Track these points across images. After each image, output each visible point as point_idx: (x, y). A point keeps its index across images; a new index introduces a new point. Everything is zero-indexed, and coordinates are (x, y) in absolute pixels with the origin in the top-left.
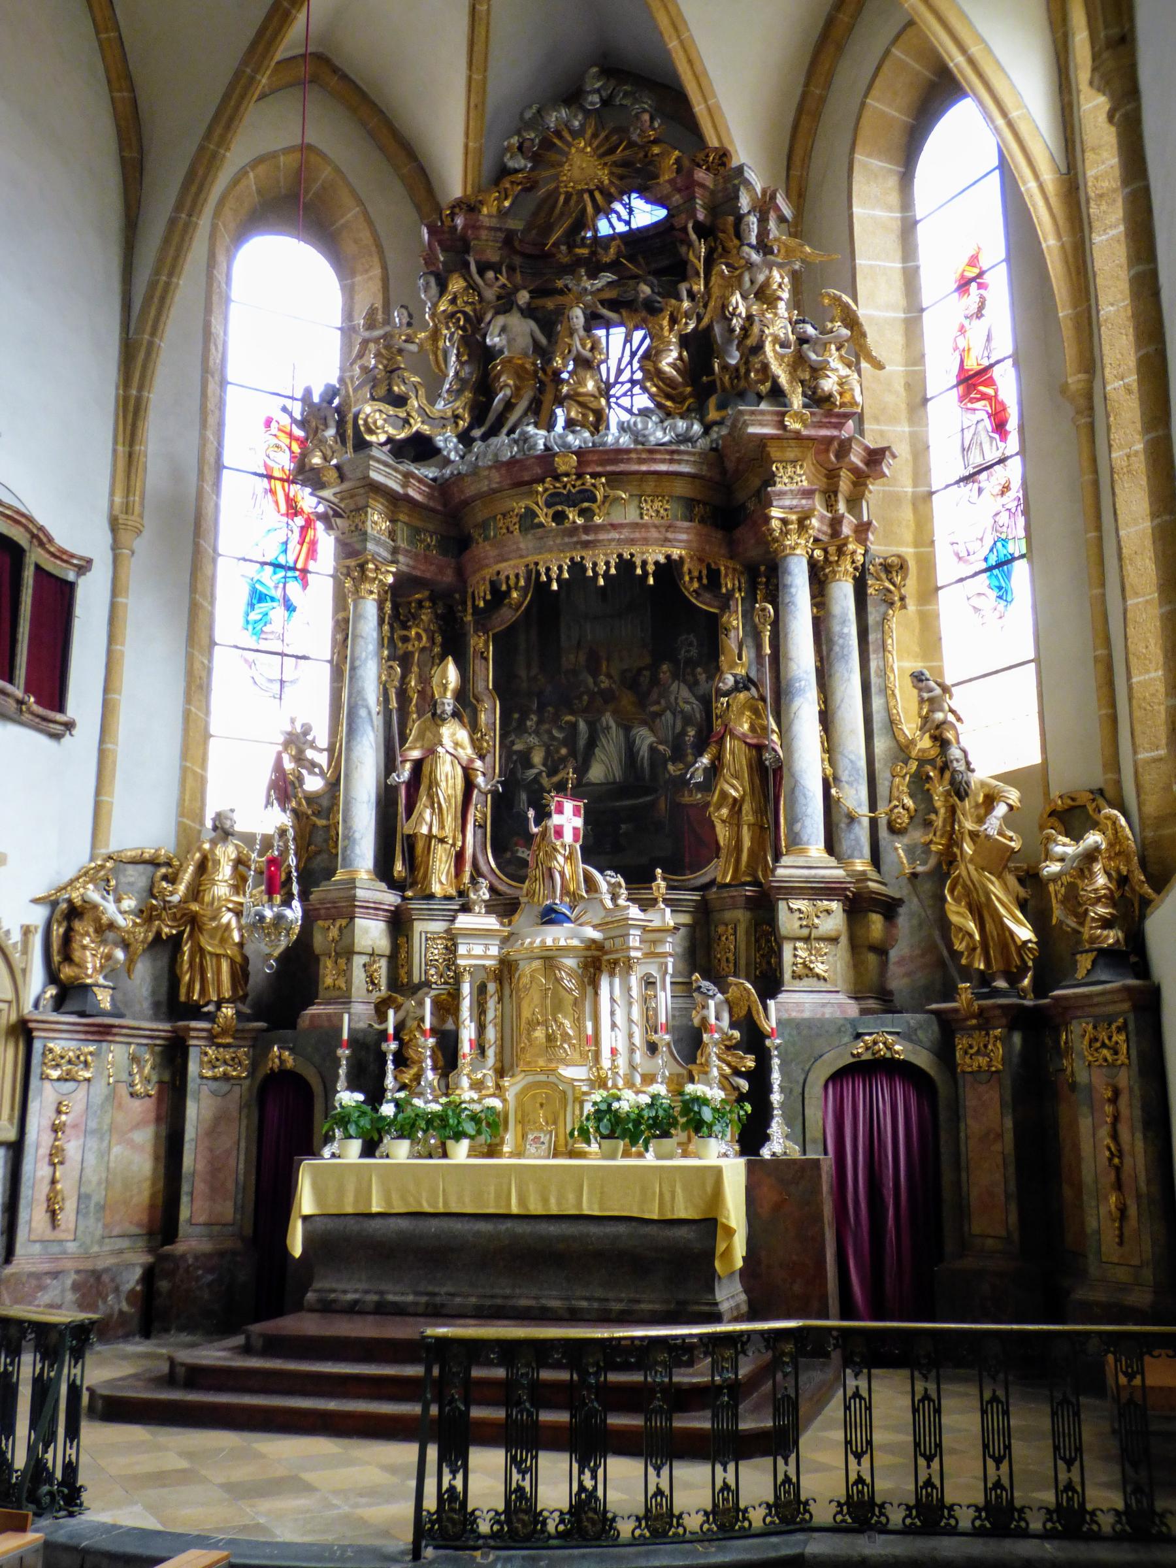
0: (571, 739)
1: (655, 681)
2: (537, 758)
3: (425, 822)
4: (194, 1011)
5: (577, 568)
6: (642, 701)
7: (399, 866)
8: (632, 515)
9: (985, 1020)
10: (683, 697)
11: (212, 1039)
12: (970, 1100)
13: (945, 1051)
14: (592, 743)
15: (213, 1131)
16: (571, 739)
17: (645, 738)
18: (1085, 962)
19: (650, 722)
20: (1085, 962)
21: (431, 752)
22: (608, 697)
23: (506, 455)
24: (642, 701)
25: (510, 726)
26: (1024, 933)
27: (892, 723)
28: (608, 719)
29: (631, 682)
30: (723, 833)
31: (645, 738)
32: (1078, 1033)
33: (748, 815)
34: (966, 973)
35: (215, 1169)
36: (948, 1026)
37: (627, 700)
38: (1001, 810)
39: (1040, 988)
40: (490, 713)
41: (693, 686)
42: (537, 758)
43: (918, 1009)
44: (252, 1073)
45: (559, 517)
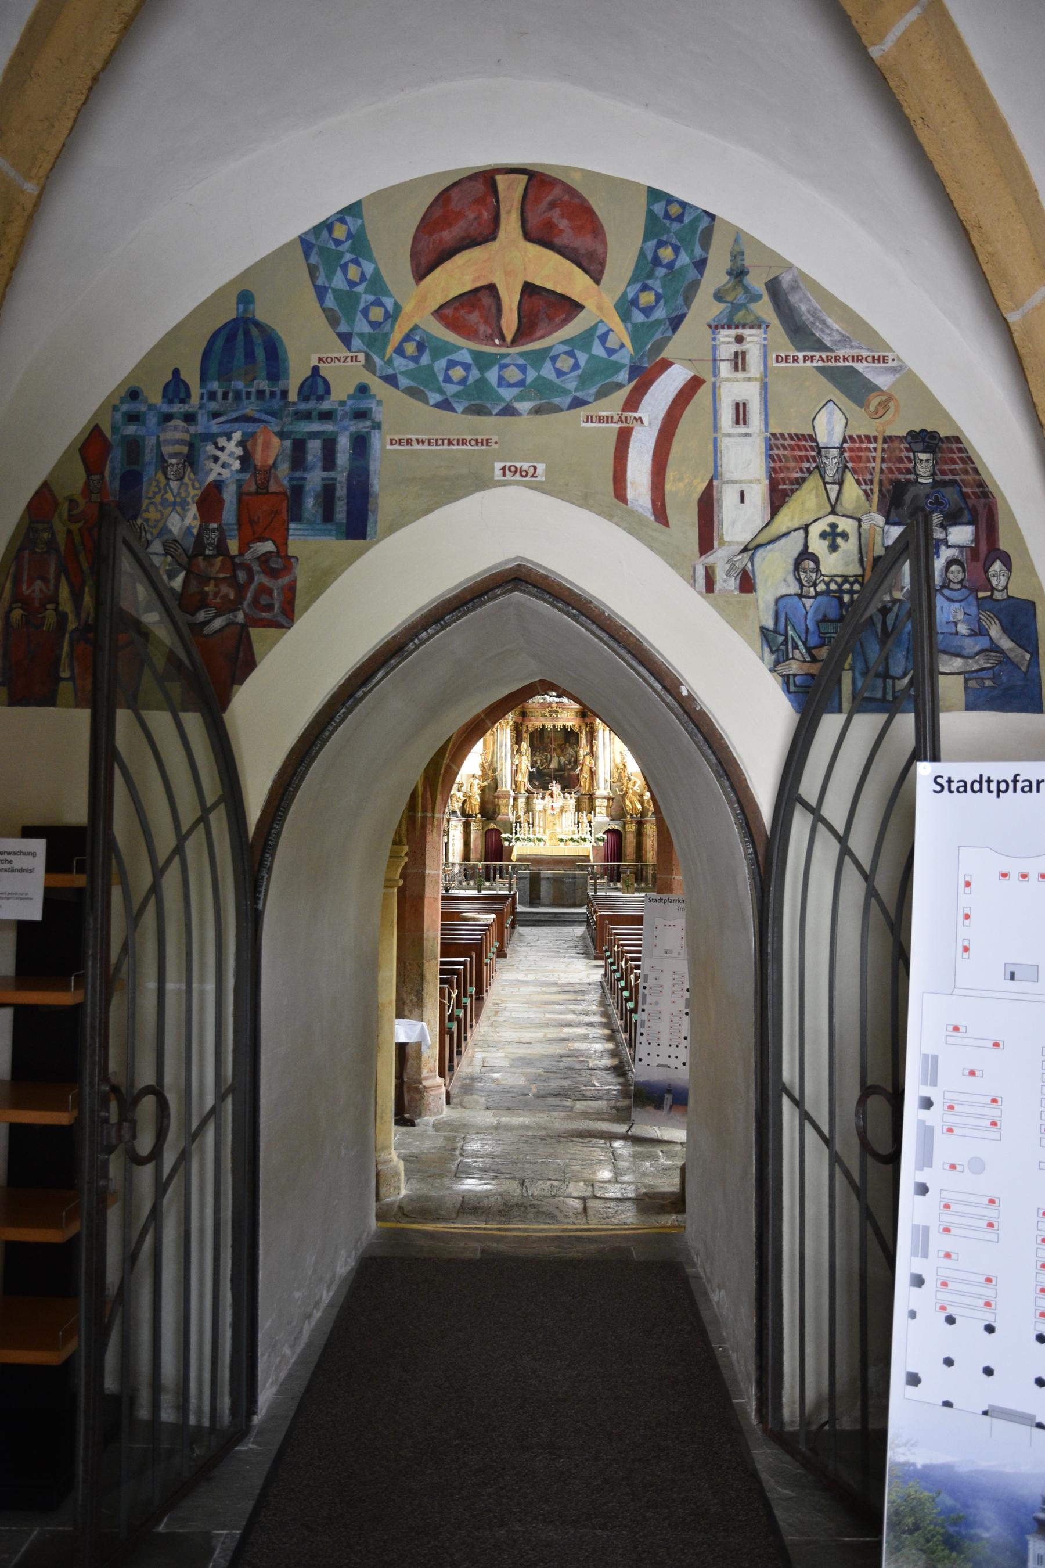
0: (546, 759)
1: (565, 747)
2: (539, 762)
3: (519, 777)
4: (470, 816)
5: (554, 726)
6: (562, 751)
7: (514, 787)
8: (566, 716)
9: (632, 823)
10: (571, 751)
11: (475, 822)
12: (628, 836)
13: (624, 827)
14: (551, 760)
15: (475, 841)
16: (546, 759)
17: (563, 759)
18: (650, 814)
19: (564, 756)
20: (650, 814)
21: (520, 762)
22: (555, 749)
23: (541, 701)
24: (562, 751)
25: (532, 755)
26: (639, 807)
27: (614, 760)
28: (555, 755)
29: (560, 746)
30: (582, 784)
31: (563, 759)
32: (648, 826)
33: (588, 781)
34: (628, 814)
35: (476, 847)
36: (625, 823)
37: (559, 751)
38: (637, 785)
39: (641, 817)
40: (529, 753)
41: (573, 749)
42: (539, 762)
43: (619, 819)
44: (483, 828)
45: (551, 715)
